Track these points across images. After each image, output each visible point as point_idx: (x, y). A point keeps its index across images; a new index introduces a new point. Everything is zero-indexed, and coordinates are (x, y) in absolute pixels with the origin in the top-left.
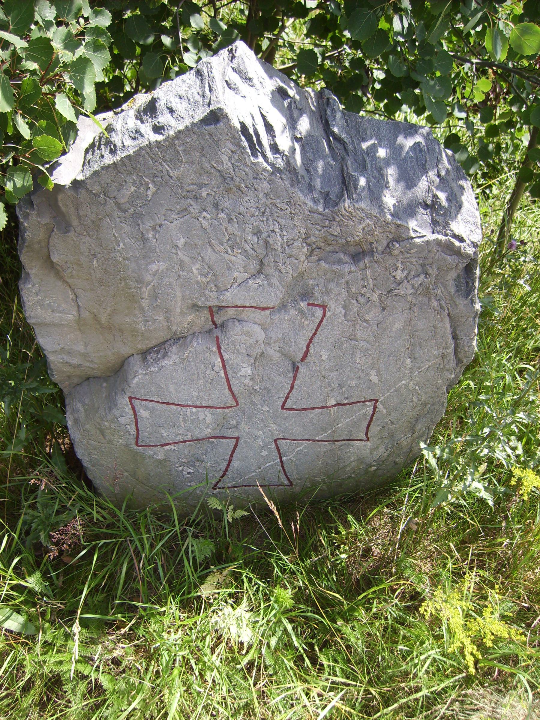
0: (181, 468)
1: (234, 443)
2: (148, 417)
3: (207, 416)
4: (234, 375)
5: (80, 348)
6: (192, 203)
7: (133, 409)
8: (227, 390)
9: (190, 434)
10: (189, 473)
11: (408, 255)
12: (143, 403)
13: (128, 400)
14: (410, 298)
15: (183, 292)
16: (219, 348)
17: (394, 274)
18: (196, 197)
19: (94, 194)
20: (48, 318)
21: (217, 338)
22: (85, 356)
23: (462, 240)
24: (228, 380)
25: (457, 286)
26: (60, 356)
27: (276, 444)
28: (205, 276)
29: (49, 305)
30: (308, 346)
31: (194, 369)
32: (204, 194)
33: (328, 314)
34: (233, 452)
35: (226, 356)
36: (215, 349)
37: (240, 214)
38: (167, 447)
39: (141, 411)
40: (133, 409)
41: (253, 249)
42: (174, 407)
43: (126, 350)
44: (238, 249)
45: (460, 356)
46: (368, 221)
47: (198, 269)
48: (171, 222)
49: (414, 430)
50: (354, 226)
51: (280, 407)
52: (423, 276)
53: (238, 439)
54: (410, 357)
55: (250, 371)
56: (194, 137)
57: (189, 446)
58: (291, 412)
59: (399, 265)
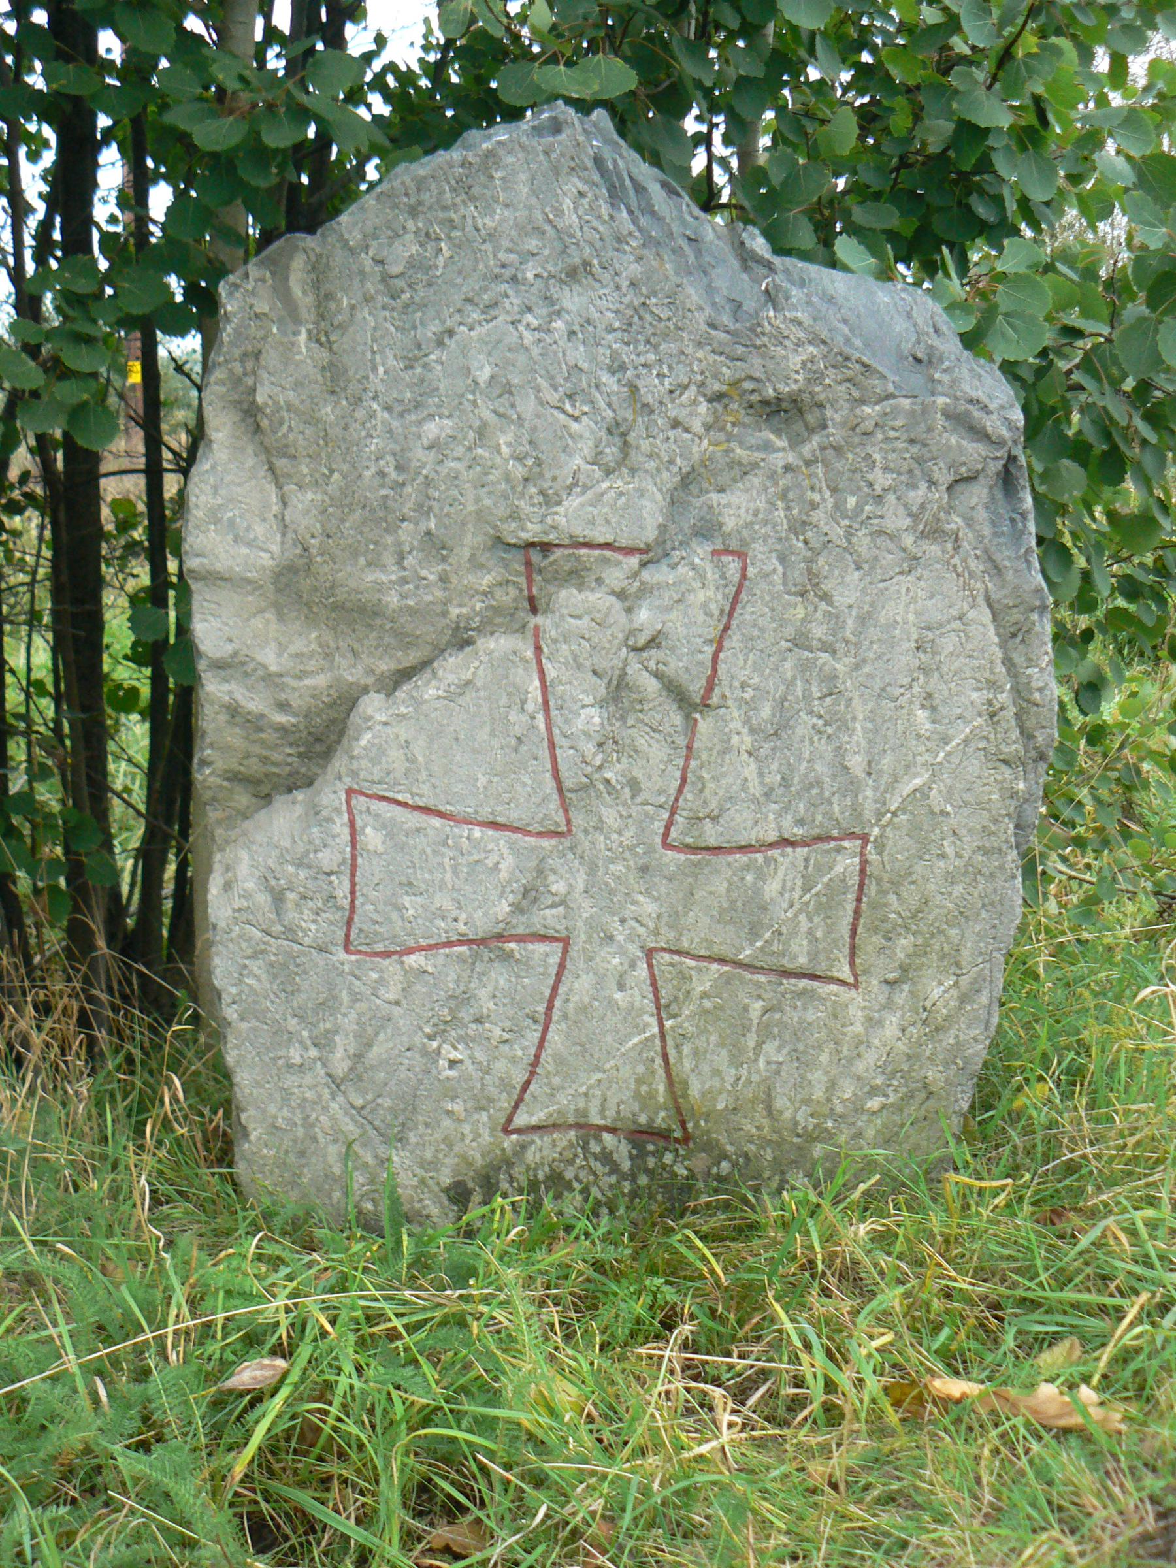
0: (435, 1044)
1: (555, 960)
2: (381, 849)
3: (501, 851)
4: (565, 728)
5: (270, 658)
6: (511, 292)
7: (352, 823)
8: (548, 775)
9: (463, 917)
10: (453, 1063)
11: (892, 434)
12: (376, 806)
13: (343, 797)
14: (908, 540)
15: (478, 500)
16: (538, 649)
17: (870, 477)
18: (514, 279)
19: (351, 249)
20: (222, 556)
21: (537, 628)
22: (270, 679)
23: (985, 408)
24: (552, 745)
25: (993, 524)
26: (226, 687)
27: (650, 966)
28: (519, 459)
29: (231, 522)
30: (715, 659)
31: (485, 710)
32: (530, 275)
33: (751, 571)
34: (555, 989)
35: (551, 672)
36: (530, 654)
37: (588, 322)
38: (412, 960)
39: (368, 830)
40: (352, 823)
41: (609, 405)
42: (437, 822)
43: (353, 674)
44: (583, 402)
45: (1028, 724)
46: (811, 349)
47: (509, 444)
48: (471, 329)
49: (958, 964)
50: (785, 357)
51: (658, 840)
52: (923, 485)
53: (566, 942)
54: (923, 706)
55: (597, 720)
56: (521, 155)
57: (461, 959)
58: (682, 857)
59: (877, 457)
